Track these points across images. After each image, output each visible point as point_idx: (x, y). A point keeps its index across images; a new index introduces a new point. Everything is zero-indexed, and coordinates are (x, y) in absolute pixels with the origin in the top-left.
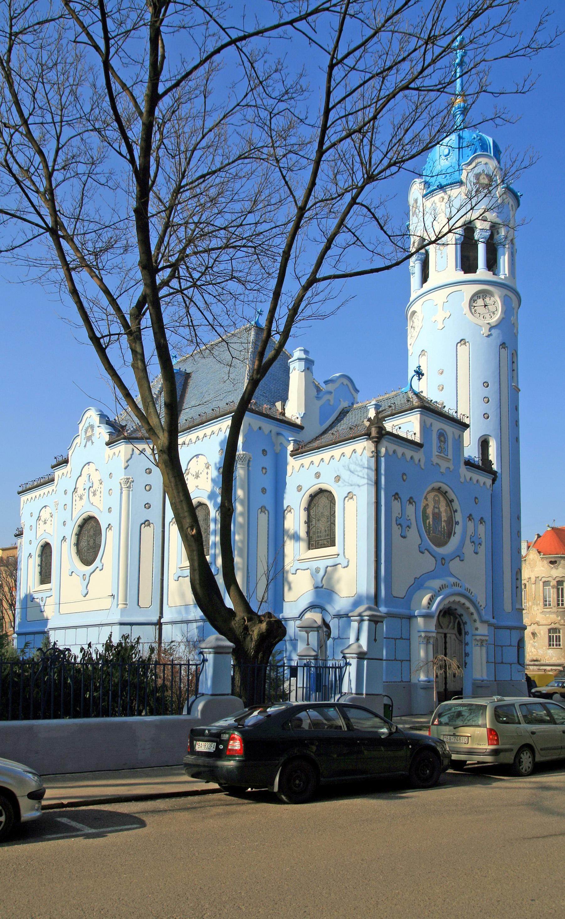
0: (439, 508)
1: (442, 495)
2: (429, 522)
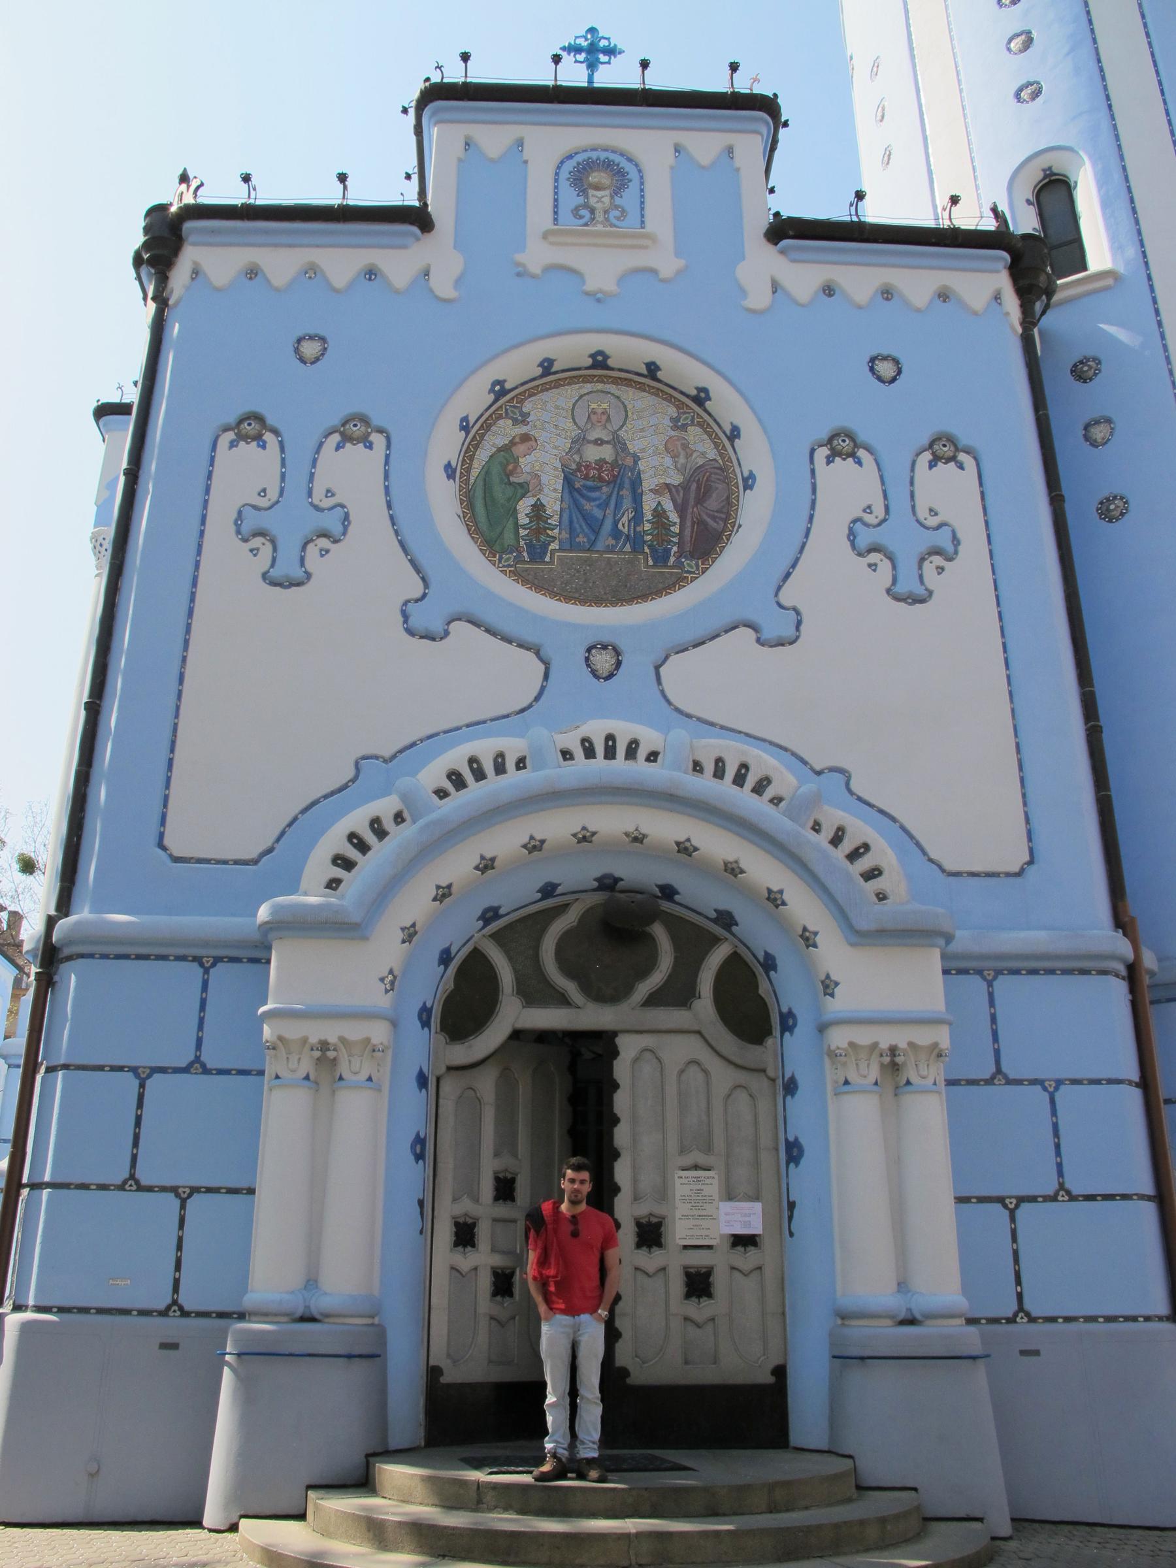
0: (618, 443)
1: (641, 387)
2: (538, 508)
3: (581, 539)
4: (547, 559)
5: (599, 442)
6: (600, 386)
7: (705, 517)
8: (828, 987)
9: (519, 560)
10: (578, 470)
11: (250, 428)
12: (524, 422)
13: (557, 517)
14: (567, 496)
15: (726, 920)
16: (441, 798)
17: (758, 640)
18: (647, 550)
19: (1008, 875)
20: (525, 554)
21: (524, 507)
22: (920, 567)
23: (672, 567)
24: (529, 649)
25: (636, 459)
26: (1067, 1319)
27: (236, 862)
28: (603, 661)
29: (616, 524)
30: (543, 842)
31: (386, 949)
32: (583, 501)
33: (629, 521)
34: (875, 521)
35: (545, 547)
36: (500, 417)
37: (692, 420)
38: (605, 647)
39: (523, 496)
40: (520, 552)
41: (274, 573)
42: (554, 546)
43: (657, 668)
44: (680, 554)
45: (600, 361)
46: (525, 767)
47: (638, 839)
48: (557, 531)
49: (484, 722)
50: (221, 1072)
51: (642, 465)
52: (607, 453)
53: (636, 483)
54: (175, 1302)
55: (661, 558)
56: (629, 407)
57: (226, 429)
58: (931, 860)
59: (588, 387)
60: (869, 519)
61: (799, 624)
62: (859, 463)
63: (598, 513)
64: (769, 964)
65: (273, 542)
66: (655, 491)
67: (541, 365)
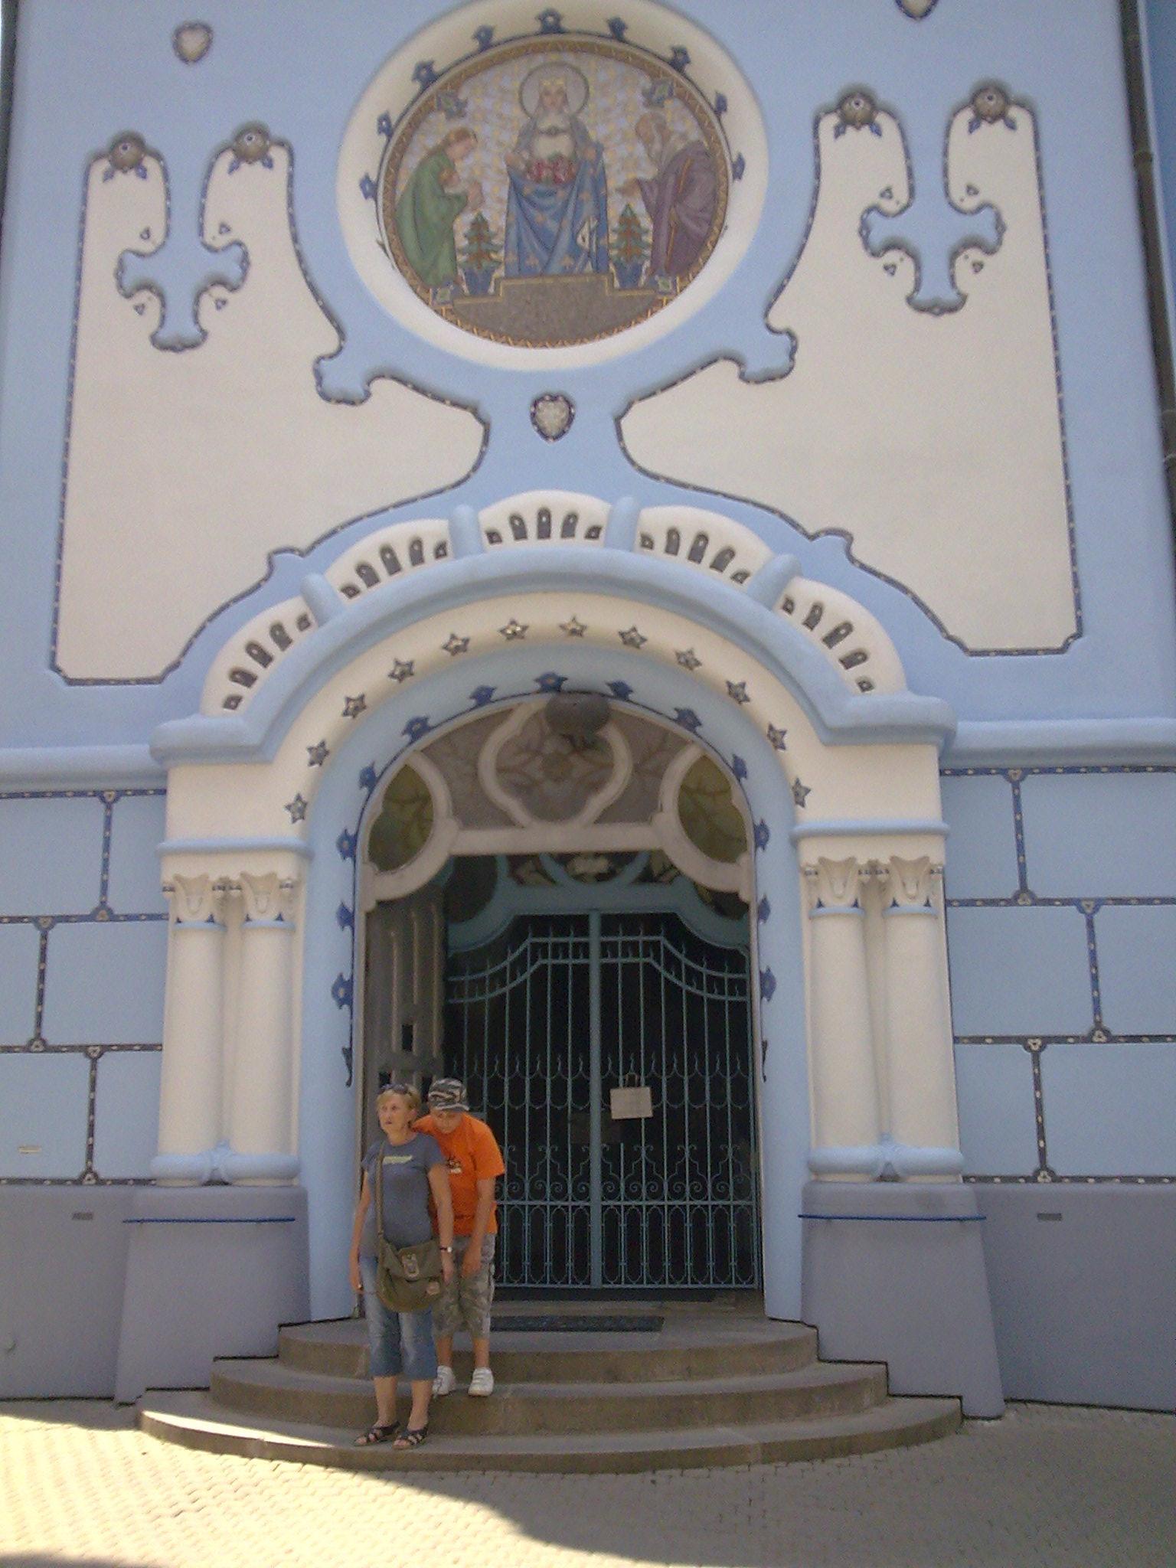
0: (577, 131)
1: (607, 54)
2: (479, 227)
3: (532, 261)
4: (491, 290)
5: (553, 132)
6: (554, 57)
7: (684, 219)
8: (799, 794)
9: (458, 294)
10: (529, 171)
11: (128, 153)
12: (461, 114)
13: (502, 236)
14: (514, 207)
15: (688, 719)
16: (350, 596)
17: (742, 377)
18: (612, 268)
19: (1048, 651)
20: (465, 287)
21: (462, 224)
22: (952, 265)
23: (644, 288)
24: (464, 407)
25: (599, 149)
26: (1099, 1179)
27: (139, 681)
28: (552, 415)
29: (574, 238)
30: (466, 641)
31: (293, 772)
32: (533, 212)
33: (591, 234)
34: (897, 208)
35: (488, 273)
36: (431, 109)
37: (671, 94)
38: (554, 398)
39: (461, 211)
40: (457, 283)
41: (165, 335)
42: (500, 273)
43: (618, 420)
44: (653, 271)
45: (551, 25)
46: (445, 554)
47: (577, 632)
48: (502, 253)
49: (414, 500)
50: (129, 918)
51: (607, 158)
52: (562, 145)
53: (600, 181)
54: (89, 1170)
55: (630, 278)
56: (590, 80)
57: (98, 157)
58: (950, 638)
59: (540, 59)
60: (890, 206)
61: (794, 350)
62: (878, 132)
63: (552, 226)
64: (740, 769)
65: (161, 296)
66: (623, 191)
67: (477, 36)
